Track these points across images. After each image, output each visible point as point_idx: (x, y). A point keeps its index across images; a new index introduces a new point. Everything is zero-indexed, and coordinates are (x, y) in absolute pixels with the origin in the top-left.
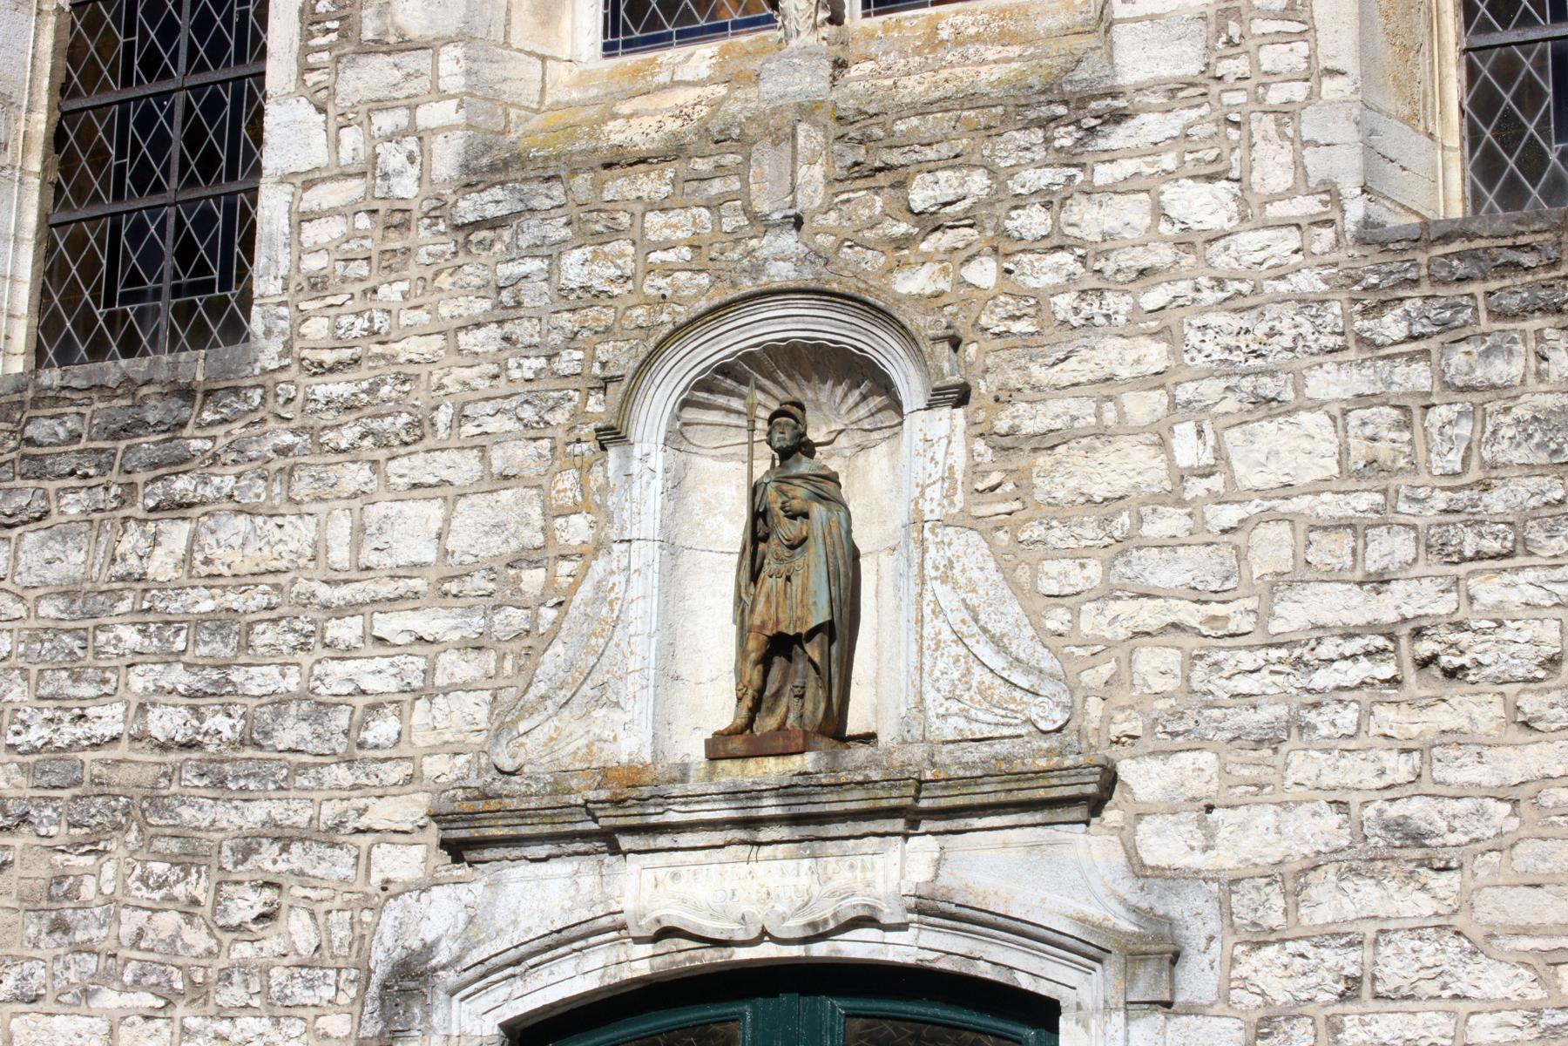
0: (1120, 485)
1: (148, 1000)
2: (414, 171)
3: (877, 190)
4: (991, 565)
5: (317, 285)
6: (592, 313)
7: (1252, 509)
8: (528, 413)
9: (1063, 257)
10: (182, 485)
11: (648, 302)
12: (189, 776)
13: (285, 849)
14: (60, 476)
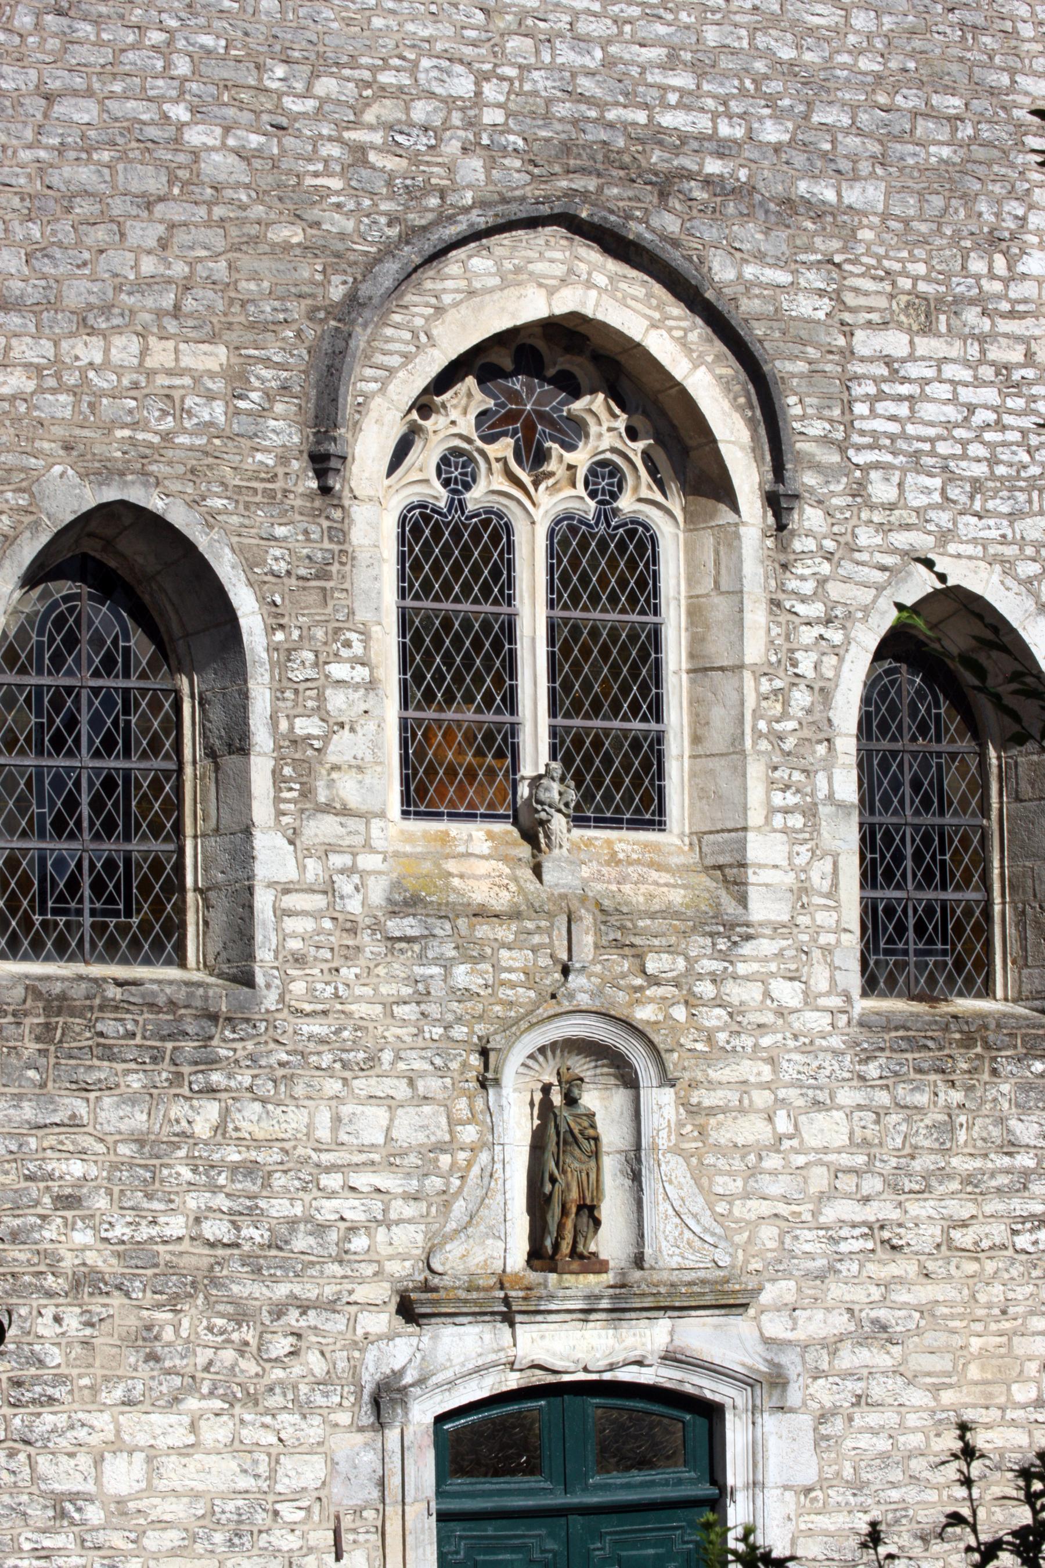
0: (751, 1139)
1: (218, 1404)
2: (359, 897)
3: (624, 956)
5: (299, 960)
6: (469, 1004)
7: (812, 1157)
8: (438, 1061)
9: (718, 1011)
10: (217, 1078)
11: (501, 1002)
12: (236, 1266)
13: (304, 1313)
14: (125, 1061)
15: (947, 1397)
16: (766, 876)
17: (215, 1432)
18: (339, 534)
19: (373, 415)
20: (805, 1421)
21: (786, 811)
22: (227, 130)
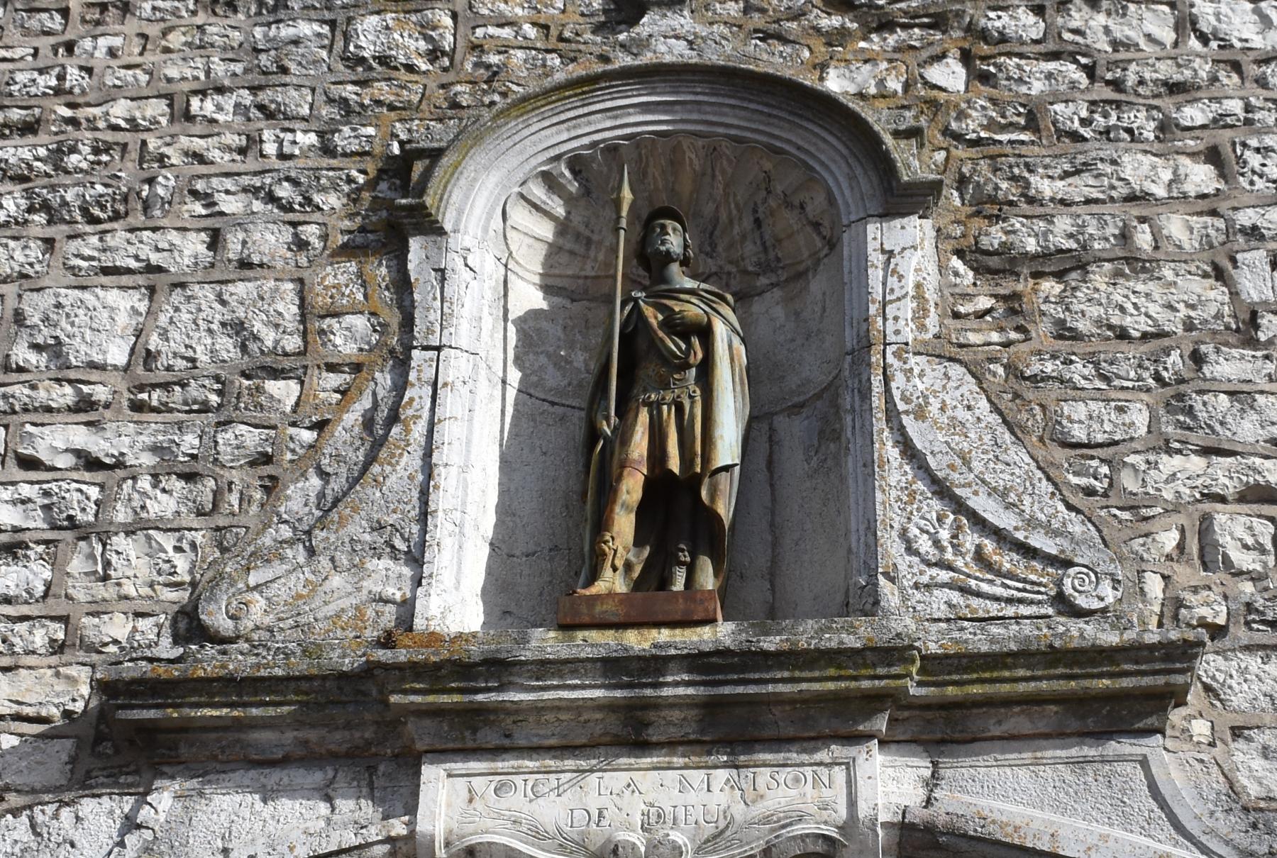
4: (983, 404)
8: (285, 191)
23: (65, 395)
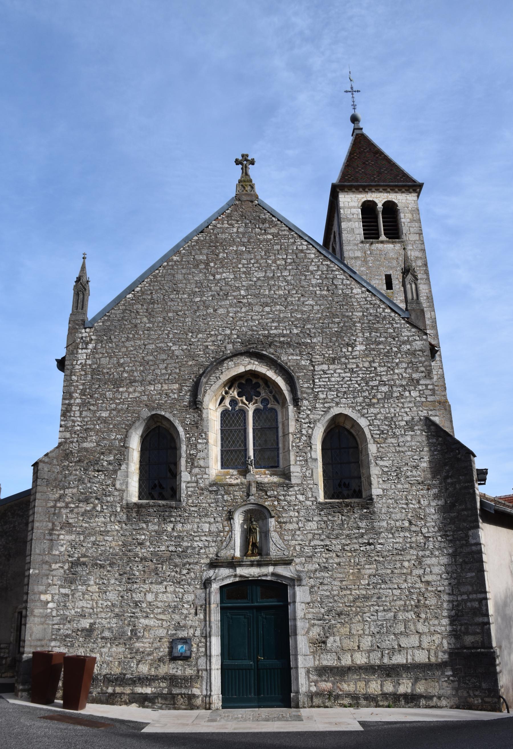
1: (171, 583)
5: (190, 496)
7: (308, 531)
10: (173, 519)
15: (344, 583)
16: (295, 474)
17: (170, 589)
18: (200, 416)
19: (208, 393)
20: (307, 588)
21: (300, 461)
22: (179, 346)
23: (203, 534)
